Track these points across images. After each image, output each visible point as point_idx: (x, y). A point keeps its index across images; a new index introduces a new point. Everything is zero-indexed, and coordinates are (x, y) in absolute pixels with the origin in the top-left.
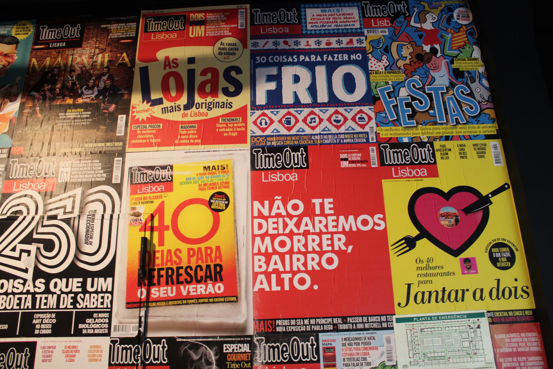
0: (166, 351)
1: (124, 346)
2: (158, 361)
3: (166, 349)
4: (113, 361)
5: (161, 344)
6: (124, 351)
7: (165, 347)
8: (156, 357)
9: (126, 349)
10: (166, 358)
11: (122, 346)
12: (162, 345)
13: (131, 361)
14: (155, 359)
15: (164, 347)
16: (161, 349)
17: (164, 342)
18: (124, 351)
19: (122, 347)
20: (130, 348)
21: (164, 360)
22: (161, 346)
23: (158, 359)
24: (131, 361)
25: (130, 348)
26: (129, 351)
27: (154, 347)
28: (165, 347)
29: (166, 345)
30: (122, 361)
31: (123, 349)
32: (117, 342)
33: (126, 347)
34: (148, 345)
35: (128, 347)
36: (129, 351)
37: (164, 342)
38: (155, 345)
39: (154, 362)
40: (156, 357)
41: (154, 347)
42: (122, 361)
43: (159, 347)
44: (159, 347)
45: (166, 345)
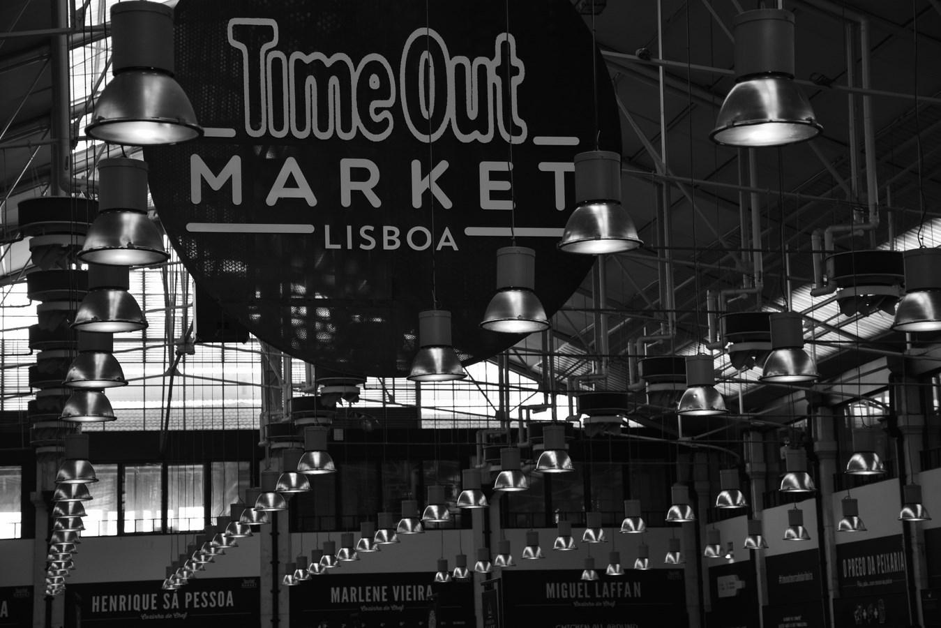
0: (519, 87)
1: (308, 59)
2: (484, 131)
3: (517, 81)
4: (256, 124)
5: (492, 57)
6: (311, 81)
7: (515, 71)
8: (472, 114)
11: (297, 55)
12: (497, 61)
13: (346, 127)
14: (466, 126)
15: (506, 71)
16: (493, 79)
17: (505, 45)
18: (311, 81)
19: (298, 62)
21: (516, 131)
22: (492, 65)
23: (481, 124)
24: (346, 127)
25: (341, 70)
26: (334, 81)
27: (460, 69)
28: (515, 71)
29: (516, 62)
30: (301, 125)
31: (302, 70)
32: (271, 39)
33: (318, 62)
34: (425, 55)
35: (328, 62)
36: (334, 81)
37: (505, 45)
40: (472, 114)
41: (460, 69)
42: (301, 125)
43: (482, 70)
44: (482, 70)
45: (516, 62)
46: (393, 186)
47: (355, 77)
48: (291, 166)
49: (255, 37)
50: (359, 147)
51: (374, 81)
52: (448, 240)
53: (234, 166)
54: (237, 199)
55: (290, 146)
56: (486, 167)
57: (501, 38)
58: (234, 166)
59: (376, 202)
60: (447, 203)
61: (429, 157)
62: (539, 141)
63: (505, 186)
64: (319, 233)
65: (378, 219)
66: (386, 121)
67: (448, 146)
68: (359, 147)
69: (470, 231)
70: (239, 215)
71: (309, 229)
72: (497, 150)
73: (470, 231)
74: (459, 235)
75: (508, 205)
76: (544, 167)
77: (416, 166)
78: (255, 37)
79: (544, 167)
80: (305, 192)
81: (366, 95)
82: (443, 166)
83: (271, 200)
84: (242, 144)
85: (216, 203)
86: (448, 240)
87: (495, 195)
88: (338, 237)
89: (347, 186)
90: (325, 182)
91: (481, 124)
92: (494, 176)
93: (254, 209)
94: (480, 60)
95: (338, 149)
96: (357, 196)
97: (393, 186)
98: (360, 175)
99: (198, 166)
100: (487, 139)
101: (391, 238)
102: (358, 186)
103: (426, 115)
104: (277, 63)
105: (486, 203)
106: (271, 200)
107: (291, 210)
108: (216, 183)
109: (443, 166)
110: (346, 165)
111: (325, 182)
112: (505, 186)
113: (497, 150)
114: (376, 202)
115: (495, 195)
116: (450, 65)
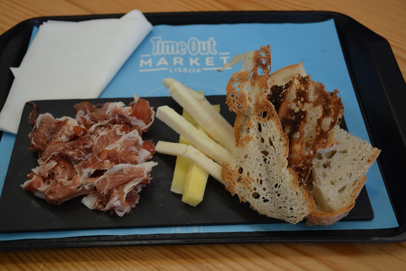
4: (155, 52)
6: (168, 46)
8: (204, 49)
10: (215, 50)
15: (212, 43)
20: (175, 44)
22: (209, 43)
23: (206, 51)
26: (173, 46)
27: (201, 45)
31: (166, 44)
34: (194, 42)
36: (173, 46)
38: (202, 42)
39: (202, 54)
40: (204, 49)
47: (178, 45)
48: (163, 59)
50: (178, 55)
51: (182, 46)
54: (150, 65)
56: (207, 59)
57: (210, 39)
59: (182, 64)
60: (198, 64)
61: (194, 58)
62: (221, 54)
63: (212, 61)
64: (168, 70)
65: (182, 67)
66: (184, 52)
67: (199, 55)
68: (178, 55)
69: (204, 69)
71: (166, 69)
72: (210, 55)
73: (204, 69)
74: (201, 69)
75: (213, 65)
76: (221, 58)
77: (191, 59)
79: (221, 58)
80: (166, 63)
81: (180, 48)
82: (197, 59)
83: (158, 64)
86: (199, 70)
87: (210, 63)
88: (173, 69)
89: (175, 63)
91: (206, 51)
92: (210, 60)
94: (206, 42)
95: (173, 56)
96: (178, 64)
100: (207, 54)
101: (185, 70)
102: (178, 62)
103: (194, 50)
104: (160, 44)
105: (208, 64)
106: (158, 64)
108: (146, 63)
109: (197, 59)
110: (175, 59)
112: (212, 61)
113: (210, 55)
114: (182, 64)
115: (210, 63)
116: (199, 43)
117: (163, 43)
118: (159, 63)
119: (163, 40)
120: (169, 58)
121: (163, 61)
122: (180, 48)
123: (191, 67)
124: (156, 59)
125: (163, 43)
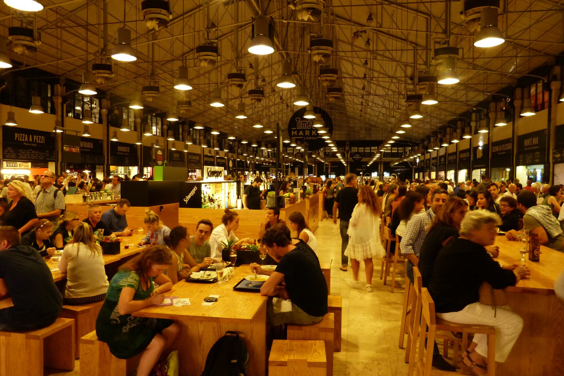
9: (304, 123)
20: (306, 122)
25: (306, 122)
31: (302, 122)
46: (311, 133)
49: (298, 120)
50: (307, 130)
52: (316, 138)
53: (296, 132)
55: (301, 130)
58: (296, 132)
65: (309, 136)
68: (307, 130)
70: (296, 136)
78: (298, 120)
80: (302, 134)
81: (308, 124)
84: (297, 130)
85: (294, 136)
86: (316, 138)
89: (306, 133)
90: (304, 133)
93: (298, 136)
97: (311, 133)
98: (307, 132)
99: (293, 132)
107: (301, 136)
111: (304, 133)
117: (301, 122)
118: (300, 134)
119: (301, 120)
120: (304, 131)
121: (301, 133)
122: (308, 124)
123: (313, 136)
124: (298, 131)
125: (301, 122)
